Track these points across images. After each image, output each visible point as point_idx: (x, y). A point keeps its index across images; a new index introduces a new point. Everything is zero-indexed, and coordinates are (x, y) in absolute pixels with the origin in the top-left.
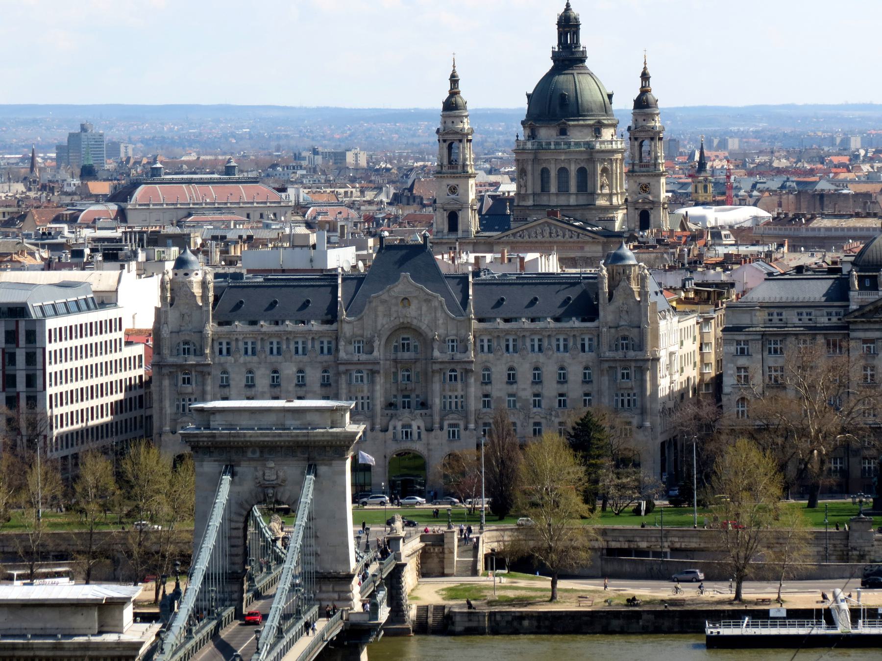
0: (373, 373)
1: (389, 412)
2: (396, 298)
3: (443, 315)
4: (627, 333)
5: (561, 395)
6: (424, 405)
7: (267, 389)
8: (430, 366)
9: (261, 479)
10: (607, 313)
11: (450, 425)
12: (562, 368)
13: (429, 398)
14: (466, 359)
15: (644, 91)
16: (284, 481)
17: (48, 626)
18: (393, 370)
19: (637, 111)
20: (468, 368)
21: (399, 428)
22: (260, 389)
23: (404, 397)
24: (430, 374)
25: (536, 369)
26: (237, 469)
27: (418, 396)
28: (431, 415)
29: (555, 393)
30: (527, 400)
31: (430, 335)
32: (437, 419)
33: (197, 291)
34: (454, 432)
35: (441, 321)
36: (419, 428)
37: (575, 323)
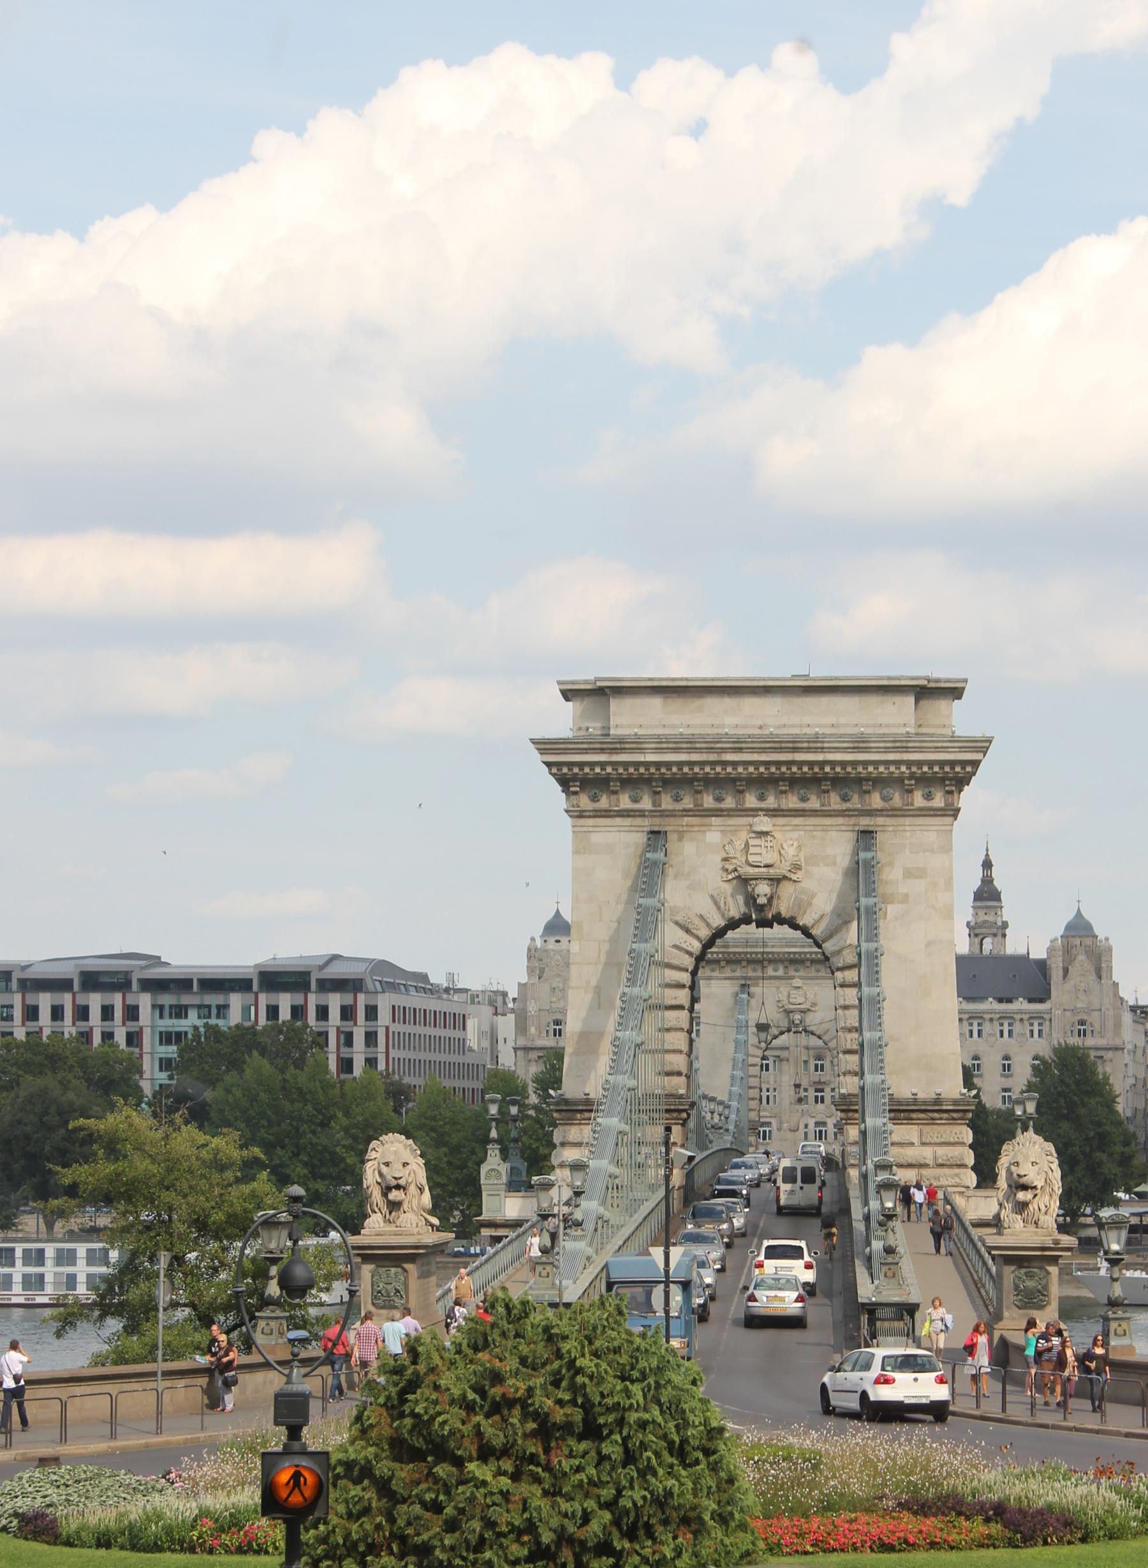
1: (800, 1107)
4: (1085, 1018)
5: (1005, 1090)
9: (785, 1002)
10: (1060, 992)
12: (1006, 1058)
15: (987, 881)
16: (814, 1004)
17: (842, 721)
18: (804, 1058)
19: (979, 904)
21: (811, 1126)
23: (816, 1091)
25: (976, 1058)
26: (753, 989)
29: (999, 1089)
37: (1021, 1005)
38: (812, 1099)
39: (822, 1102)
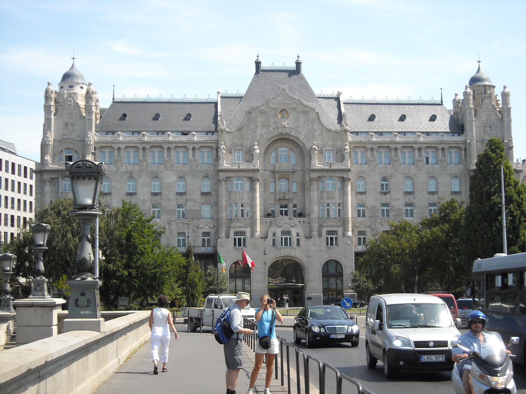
0: (252, 181)
2: (275, 109)
3: (320, 127)
6: (301, 215)
7: (148, 197)
8: (307, 175)
11: (328, 233)
13: (307, 206)
14: (344, 168)
20: (345, 176)
22: (141, 197)
23: (282, 207)
24: (307, 183)
27: (295, 206)
28: (309, 223)
29: (426, 203)
30: (400, 210)
31: (308, 146)
32: (315, 226)
33: (82, 103)
34: (332, 239)
35: (318, 133)
36: (298, 235)
38: (277, 213)
39: (286, 214)
